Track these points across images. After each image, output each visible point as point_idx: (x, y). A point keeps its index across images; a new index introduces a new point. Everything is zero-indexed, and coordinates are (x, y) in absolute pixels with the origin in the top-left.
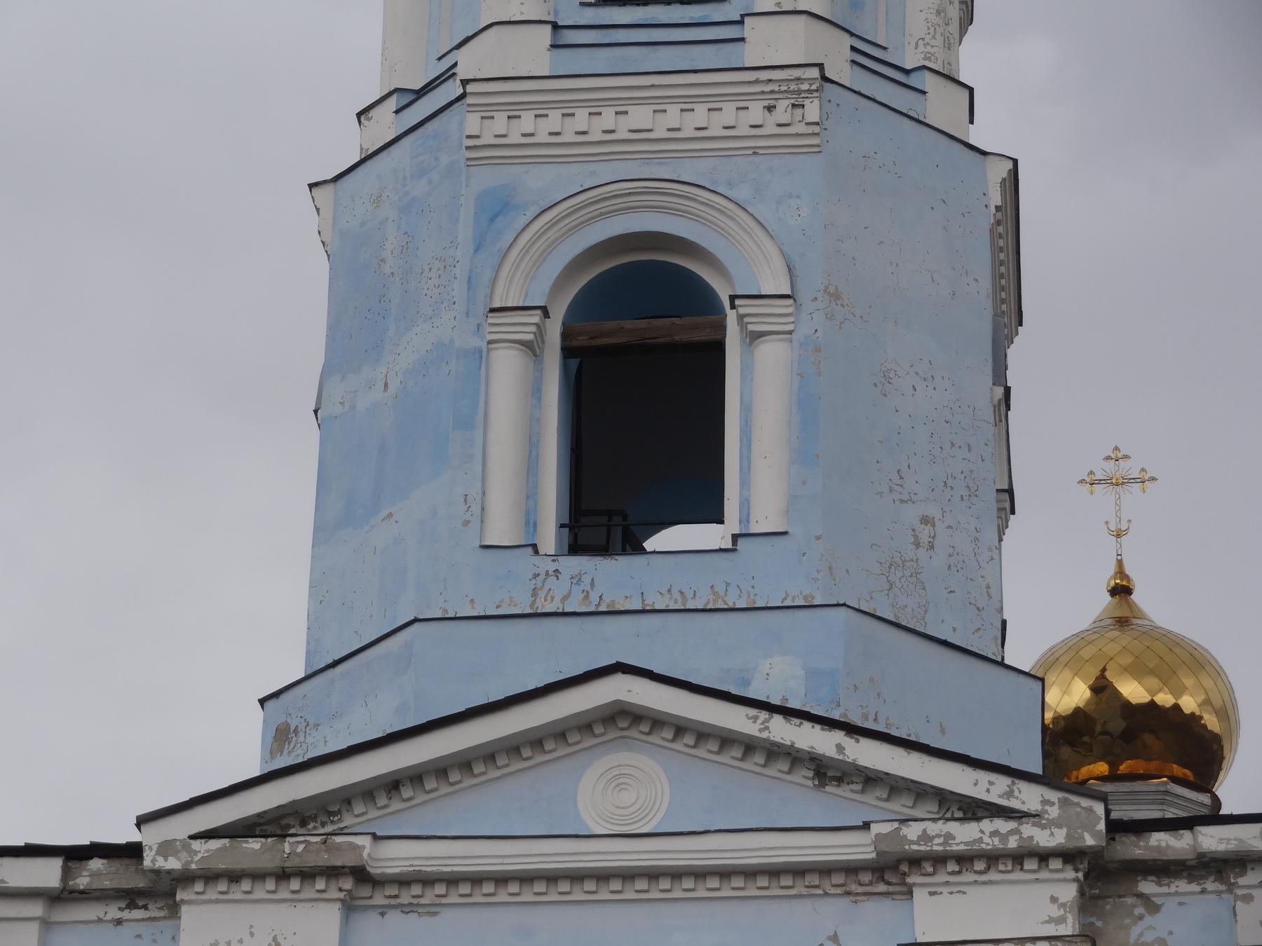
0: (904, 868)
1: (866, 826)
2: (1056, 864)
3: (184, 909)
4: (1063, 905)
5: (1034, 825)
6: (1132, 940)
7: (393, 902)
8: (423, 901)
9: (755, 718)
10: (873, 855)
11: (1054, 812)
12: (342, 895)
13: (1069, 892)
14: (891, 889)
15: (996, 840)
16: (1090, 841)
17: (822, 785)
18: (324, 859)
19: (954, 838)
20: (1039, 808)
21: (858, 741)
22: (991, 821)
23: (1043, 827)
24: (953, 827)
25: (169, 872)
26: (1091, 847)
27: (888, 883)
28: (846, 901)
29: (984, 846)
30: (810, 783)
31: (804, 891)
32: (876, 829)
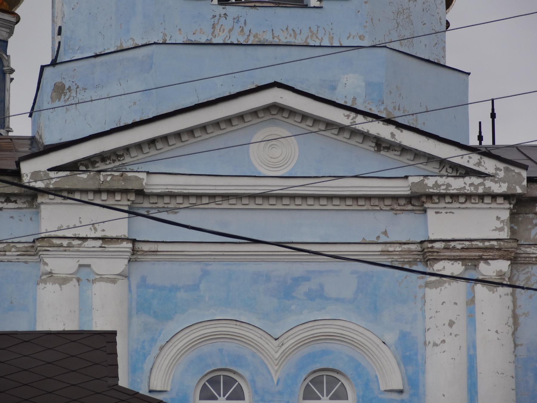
0: (424, 199)
1: (406, 177)
2: (500, 200)
3: (42, 207)
4: (503, 222)
5: (491, 181)
6: (532, 237)
7: (154, 206)
8: (170, 206)
9: (348, 116)
10: (409, 193)
11: (501, 174)
12: (129, 203)
13: (505, 215)
14: (415, 208)
15: (472, 188)
16: (519, 191)
17: (379, 150)
18: (122, 185)
19: (451, 186)
20: (494, 172)
21: (402, 131)
22: (470, 178)
23: (496, 182)
24: (451, 180)
26: (520, 193)
27: (414, 205)
28: (392, 213)
29: (466, 191)
30: (372, 149)
31: (370, 208)
32: (411, 180)
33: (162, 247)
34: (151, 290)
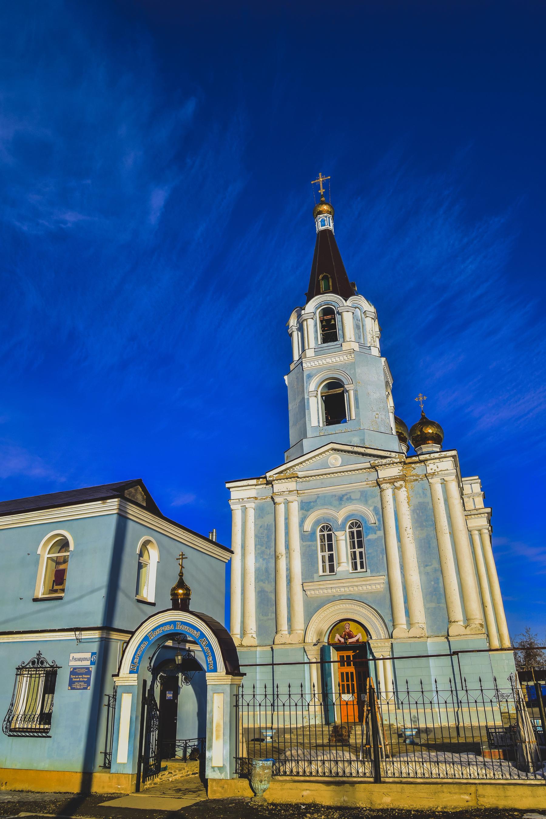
7: (303, 481)
13: (401, 468)
20: (395, 456)
25: (271, 480)
33: (306, 491)
34: (304, 504)
